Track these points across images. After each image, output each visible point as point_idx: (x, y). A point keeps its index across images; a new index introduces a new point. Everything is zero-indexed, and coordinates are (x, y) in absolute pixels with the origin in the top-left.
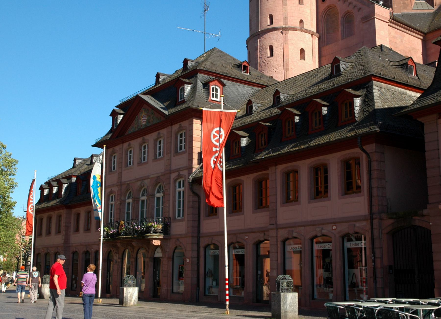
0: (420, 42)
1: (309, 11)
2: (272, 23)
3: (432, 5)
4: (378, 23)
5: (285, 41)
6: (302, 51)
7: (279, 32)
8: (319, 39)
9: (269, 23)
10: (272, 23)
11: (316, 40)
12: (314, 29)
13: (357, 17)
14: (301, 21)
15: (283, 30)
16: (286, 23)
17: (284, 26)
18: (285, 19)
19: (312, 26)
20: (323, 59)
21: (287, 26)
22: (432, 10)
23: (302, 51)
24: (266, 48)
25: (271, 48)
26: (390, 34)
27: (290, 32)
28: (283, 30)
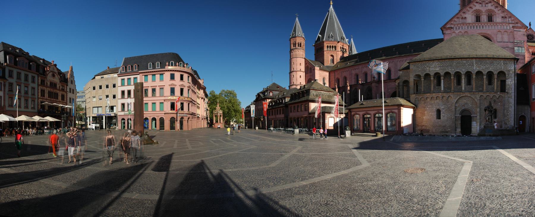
0: (328, 73)
3: (334, 64)
4: (316, 71)
5: (296, 74)
6: (300, 76)
7: (295, 72)
11: (304, 73)
12: (304, 71)
13: (312, 69)
15: (296, 71)
18: (297, 69)
19: (303, 70)
20: (306, 77)
22: (334, 65)
23: (300, 76)
25: (293, 75)
26: (319, 73)
27: (298, 72)
28: (296, 71)
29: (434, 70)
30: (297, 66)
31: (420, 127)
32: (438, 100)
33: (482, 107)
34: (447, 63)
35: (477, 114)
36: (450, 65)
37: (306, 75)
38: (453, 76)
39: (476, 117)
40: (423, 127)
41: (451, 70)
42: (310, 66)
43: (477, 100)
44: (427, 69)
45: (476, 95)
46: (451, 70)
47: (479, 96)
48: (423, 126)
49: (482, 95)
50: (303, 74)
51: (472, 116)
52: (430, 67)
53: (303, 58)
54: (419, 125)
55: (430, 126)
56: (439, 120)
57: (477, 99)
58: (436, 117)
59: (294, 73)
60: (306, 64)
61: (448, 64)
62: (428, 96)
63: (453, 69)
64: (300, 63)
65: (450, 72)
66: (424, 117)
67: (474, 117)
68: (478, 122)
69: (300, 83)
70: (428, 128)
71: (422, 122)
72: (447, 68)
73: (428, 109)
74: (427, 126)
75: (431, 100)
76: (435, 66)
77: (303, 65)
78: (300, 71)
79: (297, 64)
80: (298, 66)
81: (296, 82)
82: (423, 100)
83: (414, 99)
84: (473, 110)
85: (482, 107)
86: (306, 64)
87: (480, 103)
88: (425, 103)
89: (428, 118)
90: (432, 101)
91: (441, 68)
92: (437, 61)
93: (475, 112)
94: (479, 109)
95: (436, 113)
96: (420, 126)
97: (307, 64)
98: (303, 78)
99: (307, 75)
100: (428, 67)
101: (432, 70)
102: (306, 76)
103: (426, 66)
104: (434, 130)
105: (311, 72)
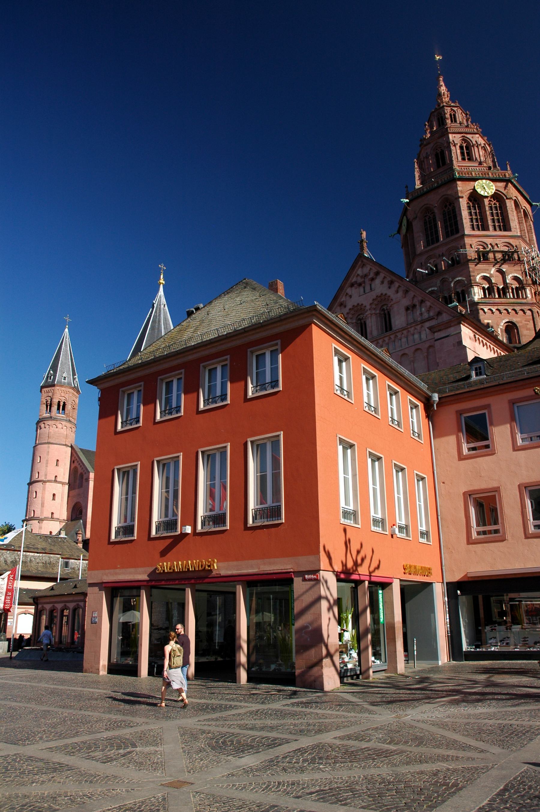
1: (62, 470)
2: (38, 478)
5: (44, 489)
6: (54, 495)
7: (41, 483)
8: (69, 486)
9: (37, 477)
10: (38, 478)
11: (67, 487)
14: (56, 476)
15: (44, 482)
16: (46, 478)
17: (44, 480)
18: (46, 475)
19: (64, 478)
20: (69, 498)
21: (46, 480)
23: (54, 495)
24: (33, 493)
28: (44, 482)
30: (47, 466)
37: (70, 492)
42: (80, 470)
50: (62, 491)
53: (66, 445)
59: (38, 487)
60: (74, 462)
64: (58, 460)
69: (52, 513)
77: (65, 464)
78: (56, 481)
79: (47, 463)
80: (48, 468)
81: (42, 512)
86: (72, 462)
97: (76, 462)
98: (62, 500)
99: (73, 492)
102: (70, 494)
105: (81, 486)
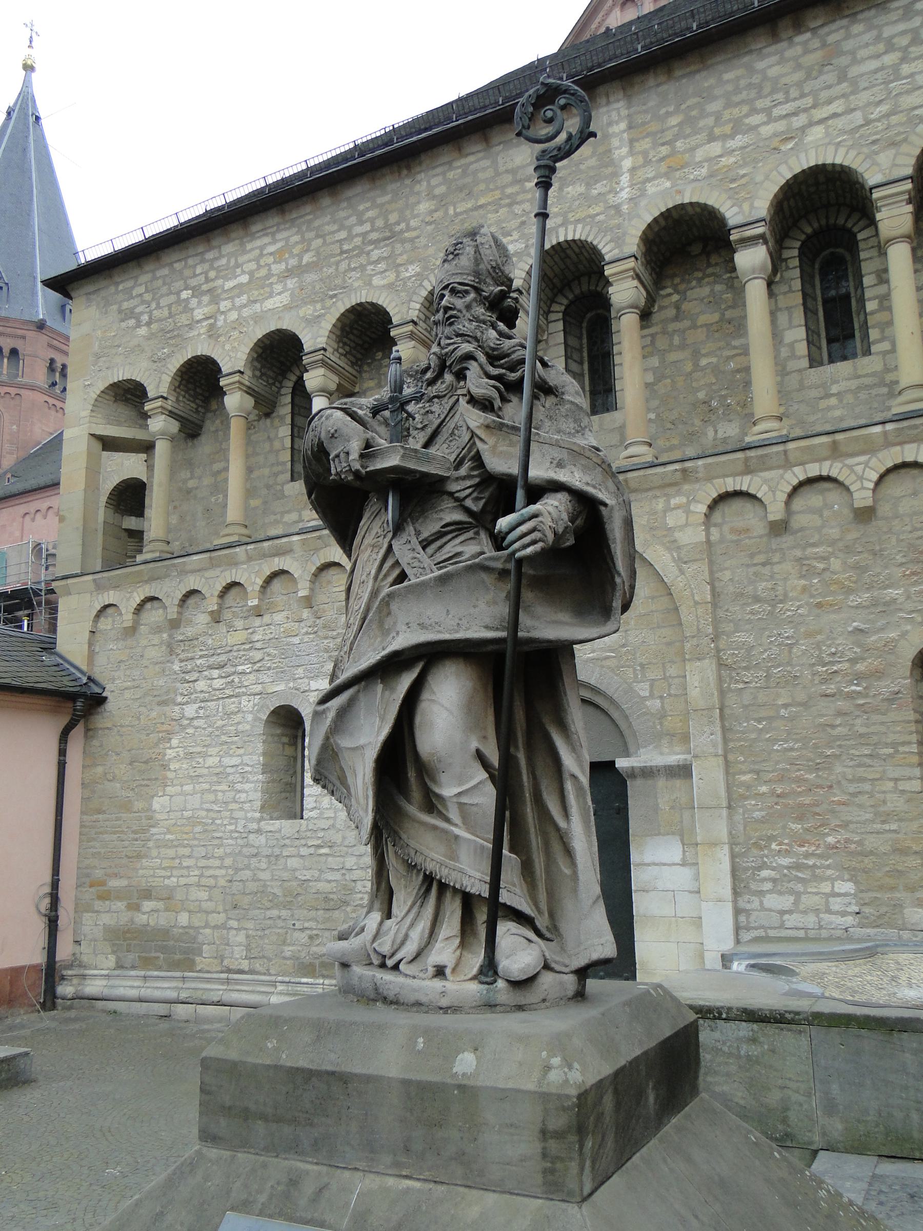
29: (246, 312)
31: (120, 905)
32: (279, 617)
33: (741, 637)
34: (361, 222)
35: (685, 738)
36: (387, 226)
38: (412, 336)
39: (683, 771)
40: (148, 905)
41: (391, 276)
43: (681, 562)
44: (198, 314)
45: (660, 505)
46: (391, 276)
47: (702, 508)
48: (147, 894)
49: (731, 484)
51: (633, 773)
52: (215, 300)
54: (114, 883)
55: (204, 895)
56: (287, 826)
57: (673, 546)
58: (257, 797)
61: (367, 227)
62: (193, 582)
63: (410, 262)
65: (383, 300)
66: (157, 804)
67: (648, 773)
68: (714, 844)
70: (183, 919)
71: (139, 856)
72: (362, 268)
73: (190, 711)
74: (179, 895)
75: (216, 618)
76: (263, 272)
82: (158, 630)
83: (88, 626)
84: (643, 689)
85: (741, 637)
87: (715, 593)
88: (171, 652)
89: (195, 801)
90: (231, 628)
91: (310, 277)
92: (272, 220)
93: (662, 715)
94: (708, 667)
95: (260, 747)
96: (118, 895)
100: (206, 299)
101: (234, 315)
103: (185, 295)
104: (241, 938)
